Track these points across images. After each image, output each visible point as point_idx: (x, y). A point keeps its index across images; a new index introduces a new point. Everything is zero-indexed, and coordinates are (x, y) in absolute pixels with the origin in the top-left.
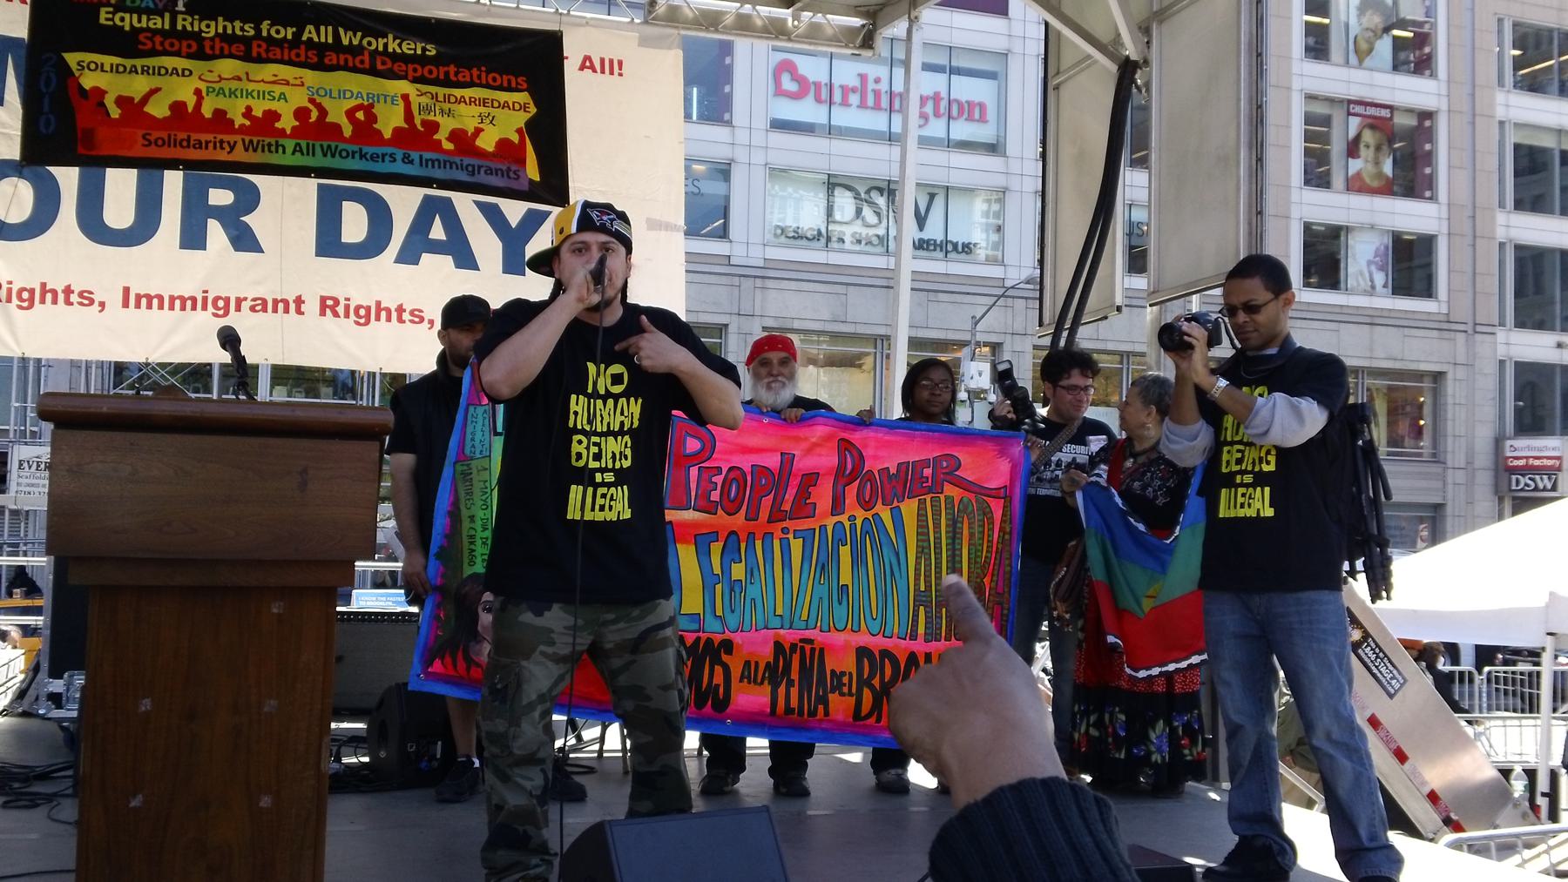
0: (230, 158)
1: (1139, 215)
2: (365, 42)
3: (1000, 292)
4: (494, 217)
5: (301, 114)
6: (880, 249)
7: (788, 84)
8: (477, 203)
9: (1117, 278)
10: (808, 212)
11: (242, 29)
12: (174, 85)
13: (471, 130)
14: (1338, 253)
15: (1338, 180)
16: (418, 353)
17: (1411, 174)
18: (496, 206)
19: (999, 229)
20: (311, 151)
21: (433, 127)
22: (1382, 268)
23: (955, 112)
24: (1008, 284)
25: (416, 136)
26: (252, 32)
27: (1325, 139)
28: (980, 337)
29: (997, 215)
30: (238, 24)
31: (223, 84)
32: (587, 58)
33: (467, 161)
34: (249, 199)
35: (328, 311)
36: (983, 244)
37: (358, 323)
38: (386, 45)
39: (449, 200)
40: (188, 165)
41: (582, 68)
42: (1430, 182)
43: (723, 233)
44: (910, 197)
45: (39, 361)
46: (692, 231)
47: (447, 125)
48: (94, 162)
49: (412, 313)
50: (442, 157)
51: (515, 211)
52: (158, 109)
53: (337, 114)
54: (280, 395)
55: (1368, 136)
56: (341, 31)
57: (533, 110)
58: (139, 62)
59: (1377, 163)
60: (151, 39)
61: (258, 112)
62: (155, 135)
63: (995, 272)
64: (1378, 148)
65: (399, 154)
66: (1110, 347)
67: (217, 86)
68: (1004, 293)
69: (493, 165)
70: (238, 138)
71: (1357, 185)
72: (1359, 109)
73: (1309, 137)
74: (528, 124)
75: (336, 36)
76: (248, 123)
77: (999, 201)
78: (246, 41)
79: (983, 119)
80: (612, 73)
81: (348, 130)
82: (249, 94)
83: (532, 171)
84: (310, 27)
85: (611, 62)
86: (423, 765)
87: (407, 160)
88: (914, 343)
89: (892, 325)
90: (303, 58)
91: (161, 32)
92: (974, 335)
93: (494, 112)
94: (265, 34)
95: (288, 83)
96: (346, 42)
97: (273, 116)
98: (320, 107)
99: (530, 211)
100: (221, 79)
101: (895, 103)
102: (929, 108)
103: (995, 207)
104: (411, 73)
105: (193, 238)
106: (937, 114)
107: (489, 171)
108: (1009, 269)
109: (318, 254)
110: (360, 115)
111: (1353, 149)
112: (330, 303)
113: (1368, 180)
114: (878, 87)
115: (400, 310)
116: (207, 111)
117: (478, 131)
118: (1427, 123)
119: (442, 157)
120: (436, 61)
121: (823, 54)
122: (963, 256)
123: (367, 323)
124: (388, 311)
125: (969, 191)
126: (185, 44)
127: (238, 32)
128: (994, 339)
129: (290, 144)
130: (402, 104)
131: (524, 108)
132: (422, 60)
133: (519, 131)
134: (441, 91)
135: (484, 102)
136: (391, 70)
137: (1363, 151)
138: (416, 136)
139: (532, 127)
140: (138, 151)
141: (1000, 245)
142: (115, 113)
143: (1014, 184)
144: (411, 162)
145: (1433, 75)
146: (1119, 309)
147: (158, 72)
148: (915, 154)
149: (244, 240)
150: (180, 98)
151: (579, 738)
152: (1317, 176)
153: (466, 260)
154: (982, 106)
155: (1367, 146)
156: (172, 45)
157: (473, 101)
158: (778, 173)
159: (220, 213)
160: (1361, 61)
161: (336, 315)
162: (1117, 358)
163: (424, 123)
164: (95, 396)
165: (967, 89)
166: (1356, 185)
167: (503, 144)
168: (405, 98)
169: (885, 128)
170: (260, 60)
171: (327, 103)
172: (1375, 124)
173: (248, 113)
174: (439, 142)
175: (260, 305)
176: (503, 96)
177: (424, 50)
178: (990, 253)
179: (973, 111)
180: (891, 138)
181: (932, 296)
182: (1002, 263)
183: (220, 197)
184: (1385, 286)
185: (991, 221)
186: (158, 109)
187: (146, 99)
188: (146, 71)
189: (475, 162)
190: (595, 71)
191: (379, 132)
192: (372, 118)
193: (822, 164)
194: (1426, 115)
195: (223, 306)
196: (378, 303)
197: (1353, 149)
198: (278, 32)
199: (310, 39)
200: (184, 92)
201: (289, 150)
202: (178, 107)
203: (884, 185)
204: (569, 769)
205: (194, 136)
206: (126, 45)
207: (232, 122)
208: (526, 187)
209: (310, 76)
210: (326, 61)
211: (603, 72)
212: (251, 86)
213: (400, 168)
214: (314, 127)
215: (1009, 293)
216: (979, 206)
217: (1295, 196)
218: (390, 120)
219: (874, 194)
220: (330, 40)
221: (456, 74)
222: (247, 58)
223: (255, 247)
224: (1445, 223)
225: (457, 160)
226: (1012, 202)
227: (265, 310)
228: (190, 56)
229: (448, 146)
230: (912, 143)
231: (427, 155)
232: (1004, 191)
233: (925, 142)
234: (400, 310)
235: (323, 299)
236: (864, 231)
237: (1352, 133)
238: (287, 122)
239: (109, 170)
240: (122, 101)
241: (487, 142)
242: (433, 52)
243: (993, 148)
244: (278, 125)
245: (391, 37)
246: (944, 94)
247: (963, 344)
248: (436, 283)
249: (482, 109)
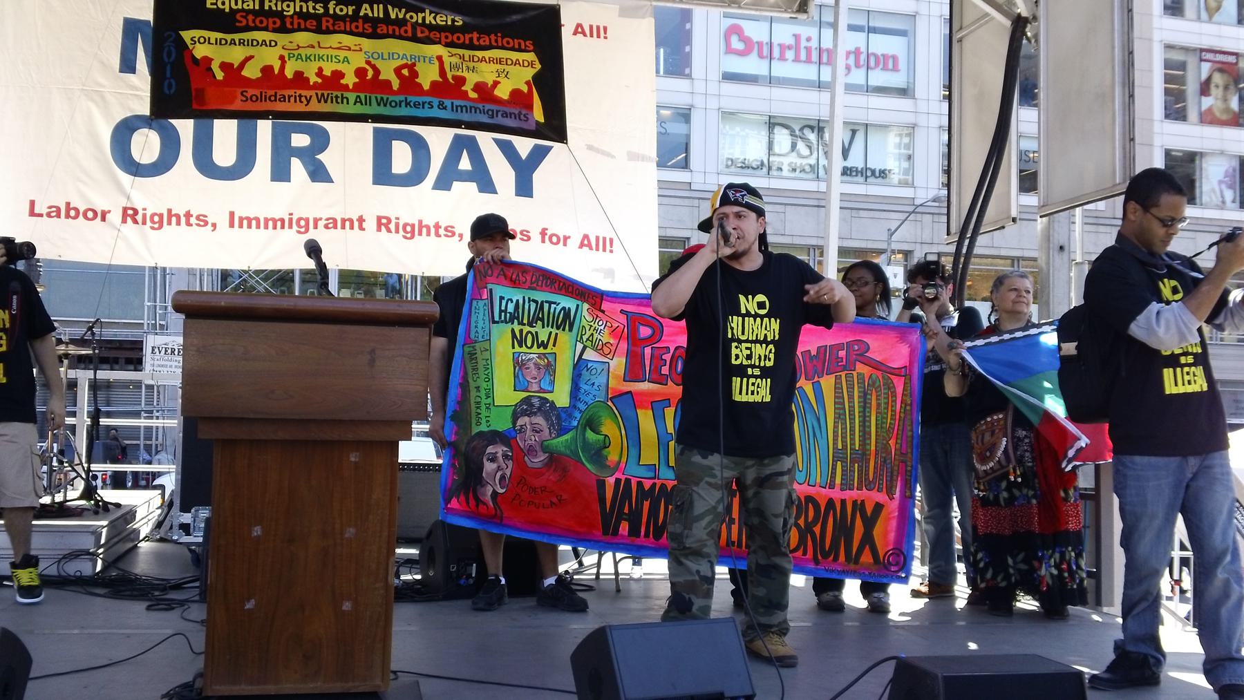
0: (309, 109)
1: (1026, 145)
2: (408, 17)
3: (911, 209)
4: (508, 151)
5: (360, 72)
6: (811, 176)
7: (737, 44)
8: (496, 141)
9: (1009, 196)
10: (752, 146)
11: (314, 8)
12: (261, 53)
13: (490, 83)
14: (1194, 173)
15: (1193, 114)
16: (450, 260)
18: (510, 142)
19: (909, 157)
20: (368, 102)
21: (461, 81)
22: (1231, 187)
23: (872, 63)
24: (918, 202)
25: (448, 88)
26: (322, 11)
27: (1181, 80)
28: (895, 246)
29: (907, 147)
30: (311, 4)
31: (300, 51)
32: (579, 25)
33: (488, 107)
34: (321, 141)
35: (383, 228)
36: (896, 170)
37: (405, 237)
38: (424, 19)
39: (473, 139)
40: (277, 115)
41: (575, 33)
43: (685, 165)
44: (838, 135)
45: (164, 269)
46: (661, 164)
47: (472, 79)
48: (205, 114)
49: (446, 229)
50: (468, 104)
51: (525, 146)
52: (252, 72)
53: (388, 73)
54: (346, 293)
55: (1218, 78)
56: (390, 7)
57: (538, 66)
58: (237, 37)
59: (1225, 100)
60: (245, 17)
61: (327, 73)
62: (251, 92)
63: (907, 192)
64: (1226, 88)
65: (436, 101)
66: (1003, 253)
67: (296, 53)
68: (914, 210)
69: (508, 110)
70: (313, 93)
71: (1209, 119)
72: (1209, 56)
73: (1168, 79)
74: (534, 78)
75: (386, 12)
76: (319, 81)
77: (909, 135)
78: (317, 17)
79: (895, 69)
80: (599, 36)
81: (396, 84)
82: (321, 58)
83: (538, 115)
84: (366, 6)
85: (598, 28)
86: (462, 582)
87: (442, 107)
88: (843, 252)
89: (825, 237)
90: (360, 30)
91: (253, 12)
92: (889, 242)
93: (507, 68)
94: (331, 12)
95: (350, 49)
96: (393, 16)
97: (338, 75)
98: (374, 67)
99: (536, 146)
100: (299, 47)
101: (825, 57)
102: (851, 61)
103: (906, 140)
104: (443, 39)
105: (280, 173)
106: (858, 66)
107: (505, 115)
108: (918, 191)
109: (374, 183)
110: (405, 72)
111: (1205, 89)
112: (384, 221)
113: (1218, 114)
114: (808, 44)
115: (437, 226)
116: (289, 73)
117: (496, 84)
119: (468, 104)
120: (465, 29)
121: (764, 18)
122: (880, 180)
123: (412, 237)
124: (428, 227)
125: (884, 127)
126: (271, 20)
127: (311, 11)
128: (906, 247)
129: (352, 96)
130: (437, 63)
131: (531, 64)
132: (452, 29)
133: (528, 83)
134: (467, 53)
135: (500, 61)
136: (428, 37)
137: (1213, 90)
138: (448, 88)
139: (538, 80)
140: (238, 105)
141: (910, 171)
142: (220, 75)
143: (922, 120)
144: (445, 108)
146: (1014, 220)
147: (251, 43)
148: (842, 98)
149: (319, 173)
150: (268, 63)
151: (581, 564)
152: (1175, 110)
153: (487, 185)
154: (895, 58)
155: (1217, 86)
156: (261, 22)
157: (491, 60)
158: (728, 115)
159: (300, 153)
160: (1211, 17)
161: (389, 231)
162: (1009, 262)
163: (454, 77)
164: (207, 293)
165: (882, 45)
166: (1208, 118)
167: (516, 93)
168: (440, 58)
169: (815, 78)
170: (328, 32)
171: (379, 64)
172: (1223, 68)
173: (320, 73)
174: (466, 92)
175: (332, 223)
176: (514, 55)
177: (453, 21)
178: (902, 177)
179: (887, 62)
180: (820, 85)
181: (854, 213)
182: (913, 186)
183: (300, 140)
184: (1234, 202)
185: (903, 151)
186: (252, 72)
187: (242, 65)
188: (242, 42)
189: (494, 107)
190: (585, 35)
191: (420, 85)
192: (414, 74)
193: (764, 108)
195: (304, 224)
196: (420, 222)
197: (1205, 89)
198: (341, 10)
199: (366, 15)
200: (270, 57)
201: (352, 101)
202: (267, 70)
203: (814, 124)
204: (574, 587)
205: (280, 92)
206: (226, 22)
207: (308, 79)
208: (533, 127)
209: (366, 43)
210: (379, 31)
211: (592, 36)
212: (322, 52)
213: (436, 113)
214: (370, 83)
215: (918, 210)
216: (892, 139)
217: (1157, 127)
218: (428, 76)
219: (807, 132)
220: (381, 15)
221: (478, 39)
222: (319, 31)
223: (329, 180)
225: (480, 106)
226: (920, 135)
227: (335, 227)
228: (275, 31)
229: (473, 95)
230: (840, 89)
231: (457, 102)
232: (914, 127)
233: (850, 88)
234: (437, 226)
235: (379, 219)
236: (799, 161)
237: (1204, 76)
238: (350, 80)
239: (216, 121)
240: (225, 66)
241: (503, 92)
242: (461, 23)
243: (904, 92)
244: (343, 82)
245: (427, 11)
246: (863, 49)
247: (880, 252)
248: (465, 205)
249: (498, 66)
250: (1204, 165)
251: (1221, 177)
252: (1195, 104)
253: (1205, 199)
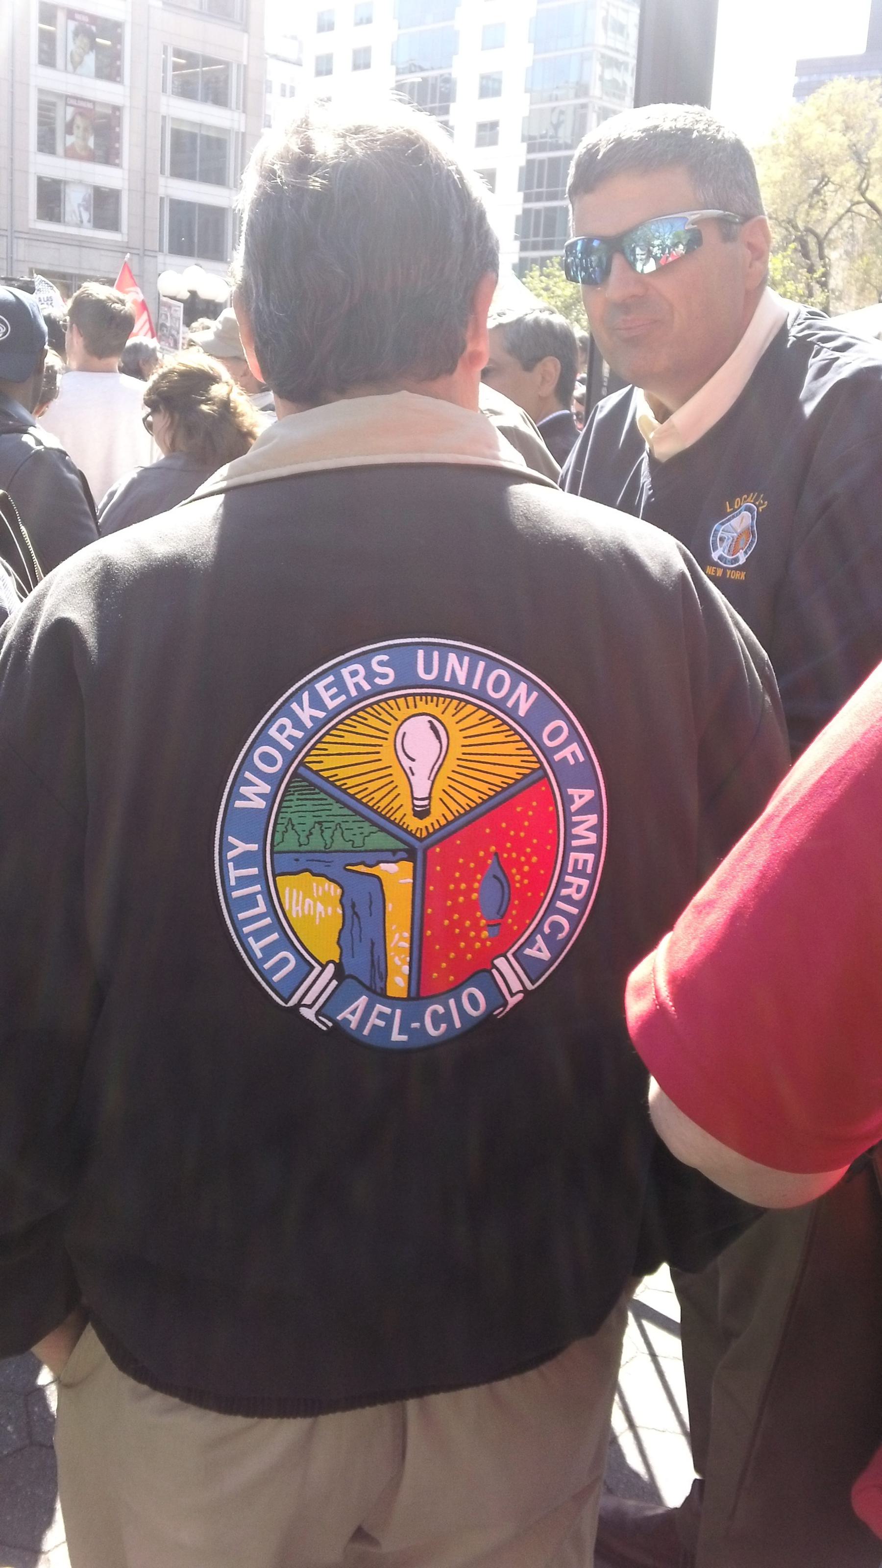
15: (60, 149)
17: (107, 152)
22: (87, 209)
42: (118, 154)
55: (79, 121)
59: (85, 139)
64: (86, 130)
111: (69, 129)
113: (78, 149)
118: (118, 113)
137: (75, 131)
145: (121, 82)
152: (46, 144)
155: (78, 127)
160: (75, 68)
166: (71, 154)
184: (89, 221)
194: (117, 109)
224: (126, 183)
237: (69, 117)
250: (67, 191)
251: (80, 201)
252: (62, 140)
253: (68, 218)
